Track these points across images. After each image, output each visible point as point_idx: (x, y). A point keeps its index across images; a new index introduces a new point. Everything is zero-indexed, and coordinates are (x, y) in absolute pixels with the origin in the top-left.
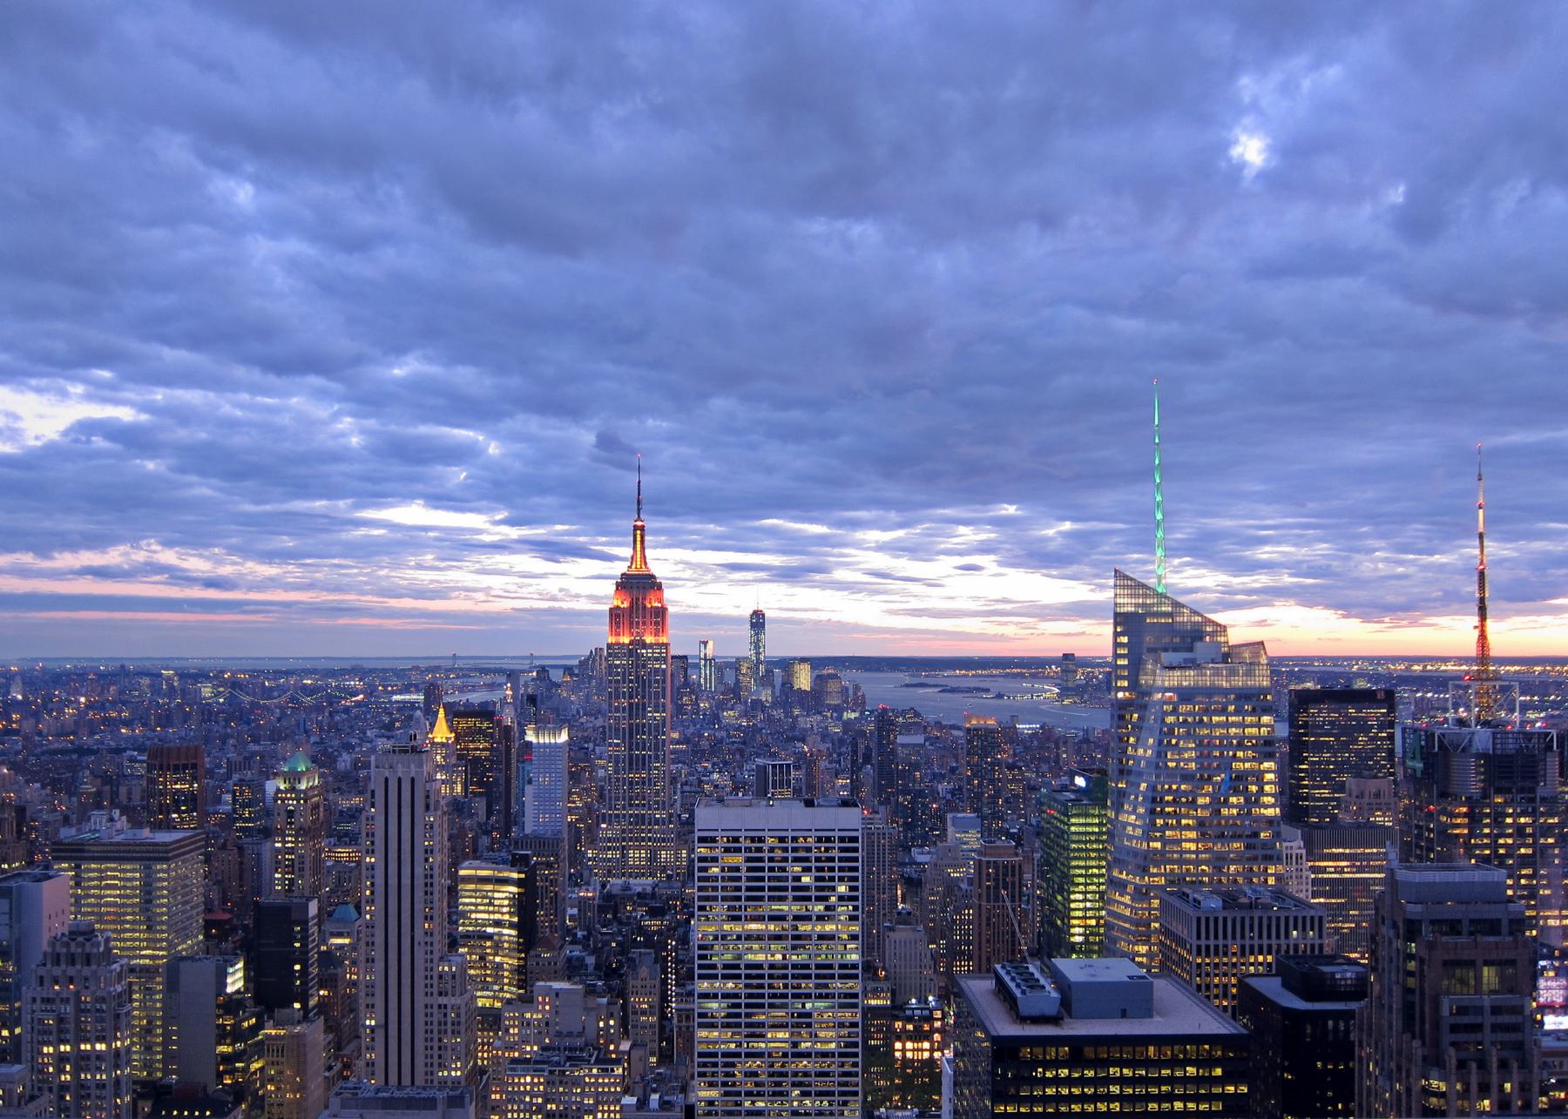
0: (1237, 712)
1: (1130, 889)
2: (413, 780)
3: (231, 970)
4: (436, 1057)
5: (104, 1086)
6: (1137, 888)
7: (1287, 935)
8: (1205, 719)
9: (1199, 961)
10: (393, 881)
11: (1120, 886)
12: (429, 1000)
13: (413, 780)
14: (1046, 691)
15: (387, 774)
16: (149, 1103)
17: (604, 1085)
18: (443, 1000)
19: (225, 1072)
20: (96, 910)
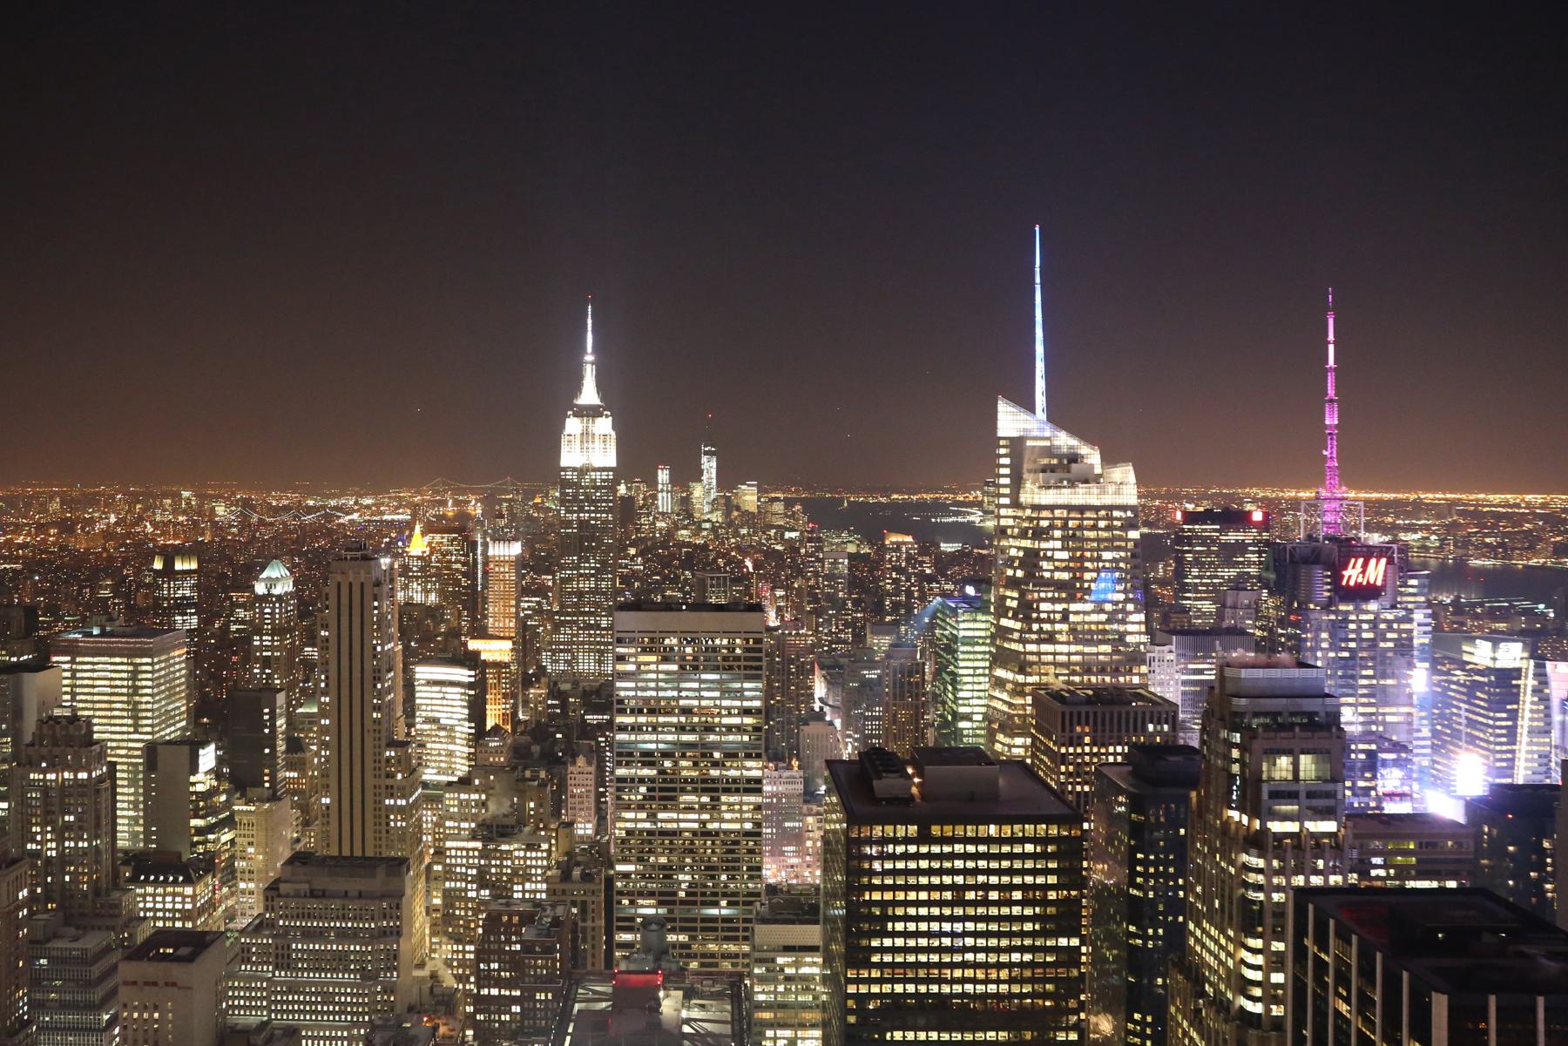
0: (1107, 528)
1: (1009, 686)
2: (362, 584)
3: (201, 752)
4: (384, 832)
5: (85, 854)
6: (1016, 684)
7: (1144, 728)
8: (1078, 533)
9: (1063, 750)
10: (345, 674)
11: (1000, 683)
12: (377, 782)
13: (362, 584)
14: (969, 514)
15: (339, 578)
16: (130, 868)
17: (531, 859)
18: (389, 782)
19: (198, 843)
20: (89, 698)
